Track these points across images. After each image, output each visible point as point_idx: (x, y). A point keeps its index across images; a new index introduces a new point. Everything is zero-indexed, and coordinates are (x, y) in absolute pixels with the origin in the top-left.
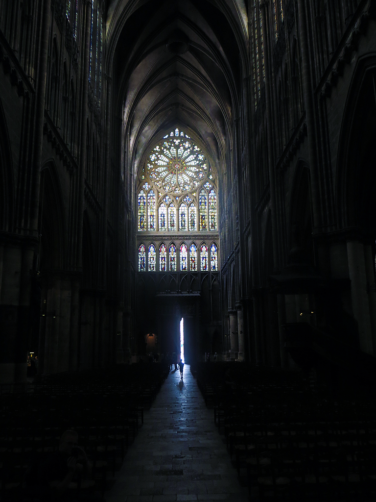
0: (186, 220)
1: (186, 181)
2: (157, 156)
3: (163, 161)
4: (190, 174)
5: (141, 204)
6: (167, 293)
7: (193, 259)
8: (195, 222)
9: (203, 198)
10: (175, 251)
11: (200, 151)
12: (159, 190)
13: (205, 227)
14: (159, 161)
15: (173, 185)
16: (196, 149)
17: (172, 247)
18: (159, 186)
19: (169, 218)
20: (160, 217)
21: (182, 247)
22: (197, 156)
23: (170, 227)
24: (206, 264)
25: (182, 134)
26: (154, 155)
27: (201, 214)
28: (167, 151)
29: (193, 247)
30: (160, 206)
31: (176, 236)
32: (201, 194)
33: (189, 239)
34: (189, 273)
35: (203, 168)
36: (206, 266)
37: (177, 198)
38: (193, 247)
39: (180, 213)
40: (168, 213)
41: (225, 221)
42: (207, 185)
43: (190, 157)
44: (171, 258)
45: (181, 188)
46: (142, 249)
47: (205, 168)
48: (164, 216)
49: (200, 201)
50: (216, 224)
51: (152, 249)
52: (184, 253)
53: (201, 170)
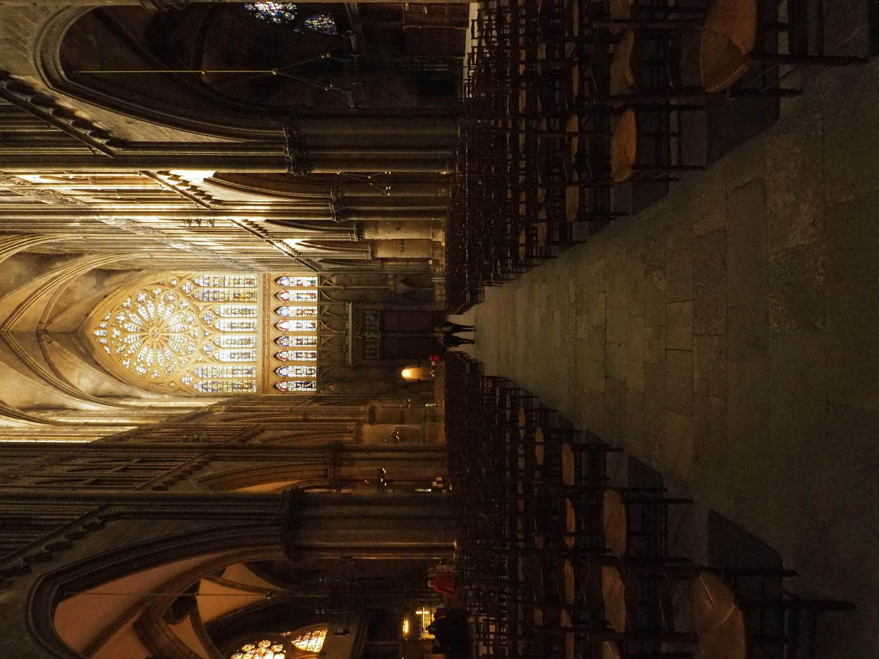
0: (241, 321)
1: (180, 320)
2: (138, 364)
3: (147, 354)
4: (168, 313)
5: (215, 387)
6: (347, 351)
7: (299, 312)
8: (244, 308)
9: (206, 295)
10: (287, 337)
11: (131, 297)
12: (193, 360)
13: (252, 294)
14: (148, 361)
15: (186, 339)
17: (282, 342)
18: (187, 360)
19: (236, 346)
20: (236, 360)
21: (282, 328)
22: (140, 302)
23: (251, 346)
24: (308, 294)
25: (103, 325)
26: (137, 369)
27: (231, 298)
29: (282, 312)
31: (263, 337)
33: (269, 317)
34: (318, 319)
35: (159, 294)
36: (312, 294)
37: (207, 334)
38: (282, 312)
39: (229, 330)
41: (235, 261)
42: (187, 288)
43: (141, 313)
44: (298, 344)
46: (284, 385)
47: (159, 290)
48: (234, 354)
49: (211, 299)
50: (247, 276)
51: (284, 372)
52: (291, 326)
53: (162, 298)
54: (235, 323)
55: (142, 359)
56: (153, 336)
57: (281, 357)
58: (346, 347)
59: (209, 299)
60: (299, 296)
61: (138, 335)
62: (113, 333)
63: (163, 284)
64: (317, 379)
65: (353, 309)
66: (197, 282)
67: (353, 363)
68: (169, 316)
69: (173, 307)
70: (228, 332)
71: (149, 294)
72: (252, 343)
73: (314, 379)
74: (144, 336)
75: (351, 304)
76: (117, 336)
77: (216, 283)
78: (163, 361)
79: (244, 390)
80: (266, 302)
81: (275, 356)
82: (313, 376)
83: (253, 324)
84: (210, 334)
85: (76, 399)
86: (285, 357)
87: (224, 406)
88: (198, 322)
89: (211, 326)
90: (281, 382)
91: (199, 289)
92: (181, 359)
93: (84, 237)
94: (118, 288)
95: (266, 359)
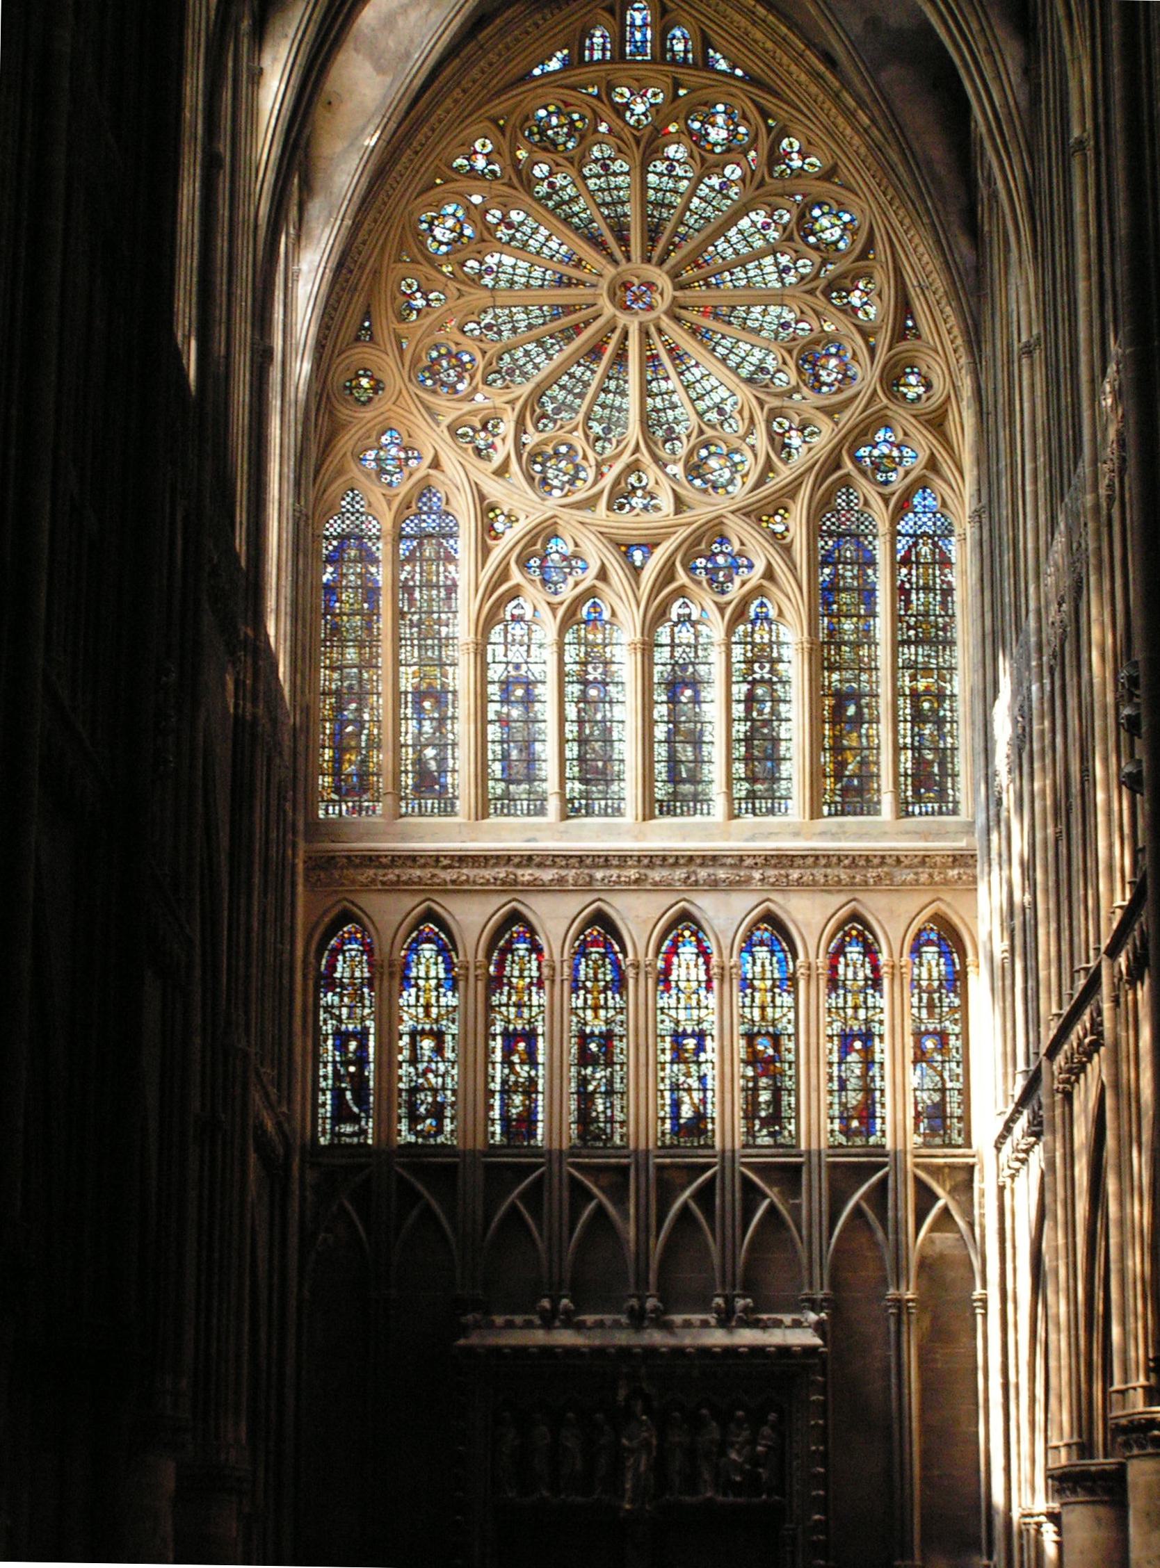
2: (476, 215)
6: (548, 1325)
11: (828, 175)
12: (494, 490)
14: (491, 261)
16: (797, 163)
18: (497, 459)
21: (674, 951)
23: (575, 787)
24: (868, 1090)
26: (450, 209)
29: (762, 953)
31: (623, 860)
42: (885, 449)
43: (744, 223)
44: (584, 1038)
48: (529, 701)
54: (696, 700)
55: (503, 233)
56: (626, 286)
57: (509, 949)
58: (567, 1311)
59: (825, 563)
60: (858, 1045)
61: (627, 208)
63: (900, 333)
64: (387, 1152)
65: (784, 1351)
66: (916, 500)
67: (470, 1351)
68: (733, 360)
72: (586, 795)
73: (386, 1127)
74: (623, 240)
75: (818, 1341)
76: (621, 110)
79: (328, 753)
80: (819, 873)
81: (515, 917)
82: (404, 1126)
83: (696, 798)
85: (312, 29)
86: (511, 970)
87: (261, 710)
88: (703, 510)
89: (682, 578)
90: (368, 950)
91: (880, 515)
92: (502, 428)
93: (1080, 142)
94: (873, 120)
95: (501, 873)
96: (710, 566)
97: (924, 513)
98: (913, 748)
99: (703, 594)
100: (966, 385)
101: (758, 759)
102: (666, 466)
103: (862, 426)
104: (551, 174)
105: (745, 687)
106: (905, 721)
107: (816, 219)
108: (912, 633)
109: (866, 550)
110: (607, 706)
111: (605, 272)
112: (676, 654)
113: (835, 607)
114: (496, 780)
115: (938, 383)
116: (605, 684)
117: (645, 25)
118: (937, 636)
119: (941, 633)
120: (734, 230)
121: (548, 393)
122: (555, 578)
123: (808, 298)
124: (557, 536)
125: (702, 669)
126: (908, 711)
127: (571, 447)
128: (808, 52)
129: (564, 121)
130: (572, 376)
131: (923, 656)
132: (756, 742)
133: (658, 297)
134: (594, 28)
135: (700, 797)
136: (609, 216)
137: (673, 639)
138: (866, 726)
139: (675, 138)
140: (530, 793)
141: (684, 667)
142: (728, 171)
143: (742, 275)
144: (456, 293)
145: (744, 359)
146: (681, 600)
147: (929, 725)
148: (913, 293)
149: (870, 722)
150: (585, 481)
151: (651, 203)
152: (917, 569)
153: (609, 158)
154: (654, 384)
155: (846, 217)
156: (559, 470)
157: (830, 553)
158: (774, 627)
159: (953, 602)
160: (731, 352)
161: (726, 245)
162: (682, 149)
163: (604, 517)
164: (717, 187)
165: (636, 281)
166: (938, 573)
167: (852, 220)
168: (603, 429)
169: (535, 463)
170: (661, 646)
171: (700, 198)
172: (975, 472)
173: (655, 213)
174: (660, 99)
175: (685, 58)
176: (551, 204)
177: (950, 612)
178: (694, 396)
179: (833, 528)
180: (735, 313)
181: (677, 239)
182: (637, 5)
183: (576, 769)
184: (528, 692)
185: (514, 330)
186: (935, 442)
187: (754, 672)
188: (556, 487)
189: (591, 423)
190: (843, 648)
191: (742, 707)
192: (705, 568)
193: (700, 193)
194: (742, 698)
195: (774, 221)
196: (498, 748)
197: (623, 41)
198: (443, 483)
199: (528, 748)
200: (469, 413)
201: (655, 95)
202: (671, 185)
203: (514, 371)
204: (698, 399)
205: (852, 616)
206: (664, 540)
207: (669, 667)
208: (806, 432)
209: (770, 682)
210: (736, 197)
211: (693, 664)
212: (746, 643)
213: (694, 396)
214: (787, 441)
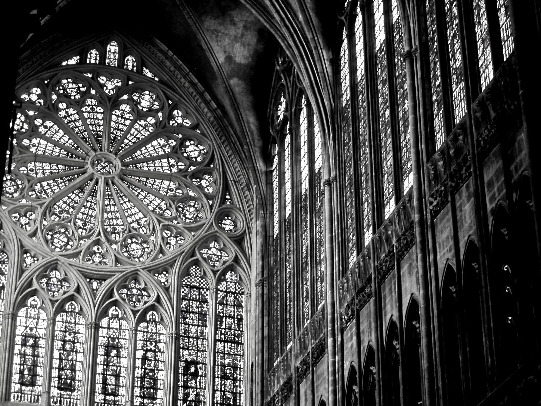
1: (135, 225)
8: (159, 384)
11: (195, 127)
12: (28, 243)
14: (35, 141)
16: (180, 121)
19: (56, 354)
22: (182, 144)
23: (55, 392)
25: (130, 62)
28: (71, 111)
30: (22, 304)
32: (186, 280)
35: (200, 187)
37: (95, 284)
39: (102, 341)
40: (53, 336)
42: (214, 251)
43: (155, 143)
45: (114, 246)
48: (35, 346)
53: (191, 193)
54: (118, 356)
59: (184, 299)
61: (101, 128)
62: (111, 76)
63: (223, 201)
66: (228, 276)
69: (168, 214)
70: (96, 337)
71: (201, 167)
76: (102, 86)
77: (227, 322)
78: (32, 174)
84: (94, 293)
92: (33, 217)
96: (129, 293)
97: (231, 282)
98: (221, 391)
99: (126, 305)
100: (256, 226)
101: (147, 388)
102: (112, 244)
103: (205, 238)
104: (67, 108)
105: (142, 352)
106: (218, 377)
107: (188, 146)
108: (223, 336)
109: (202, 295)
110: (74, 353)
111: (90, 154)
112: (110, 333)
113: (187, 320)
114: (16, 383)
115: (240, 225)
116: (74, 342)
117: (115, 52)
118: (234, 339)
119: (236, 338)
120: (150, 145)
121: (58, 204)
122: (53, 290)
123: (184, 179)
124: (56, 270)
125: (122, 342)
126: (219, 373)
127: (67, 230)
128: (191, 73)
129: (74, 86)
130: (69, 198)
131: (227, 348)
132: (146, 379)
133: (114, 169)
134: (92, 49)
135: (117, 403)
136: (93, 130)
137: (109, 325)
138: (199, 378)
139: (126, 102)
140: (32, 391)
141: (113, 339)
142: (149, 119)
143: (152, 165)
144: (18, 153)
145: (151, 202)
146: (114, 308)
147: (229, 381)
148: (231, 184)
149: (202, 376)
150: (72, 246)
151: (113, 128)
152: (226, 307)
153: (95, 105)
154: (109, 207)
155: (201, 148)
156: (60, 240)
157: (186, 295)
158: (158, 325)
159: (242, 325)
160: (145, 198)
161: (146, 151)
162: (128, 107)
163: (81, 263)
164: (143, 126)
165: (104, 160)
166: (236, 310)
167: (204, 149)
168: (82, 224)
169: (48, 234)
170: (103, 328)
171: (135, 129)
172: (261, 263)
173: (115, 132)
174: (120, 84)
175: (132, 70)
176: (66, 121)
177: (241, 329)
178: (127, 215)
179: (188, 283)
180: (148, 181)
181: (123, 145)
182: (112, 44)
183: (56, 382)
184: (35, 341)
185: (44, 173)
186: (238, 250)
187: (147, 346)
188: (58, 247)
189: (77, 220)
190: (190, 339)
191: (140, 361)
192: (127, 294)
193: (135, 127)
194: (141, 357)
195: (169, 144)
196: (18, 367)
197: (105, 58)
198: (4, 237)
199: (33, 369)
200: (19, 207)
201: (118, 82)
202: (122, 122)
203: (42, 192)
204: (128, 216)
205: (195, 325)
206: (109, 278)
207: (106, 339)
208: (178, 239)
209: (154, 351)
210: (152, 131)
211: (118, 338)
212: (144, 332)
213: (127, 215)
214: (169, 241)
